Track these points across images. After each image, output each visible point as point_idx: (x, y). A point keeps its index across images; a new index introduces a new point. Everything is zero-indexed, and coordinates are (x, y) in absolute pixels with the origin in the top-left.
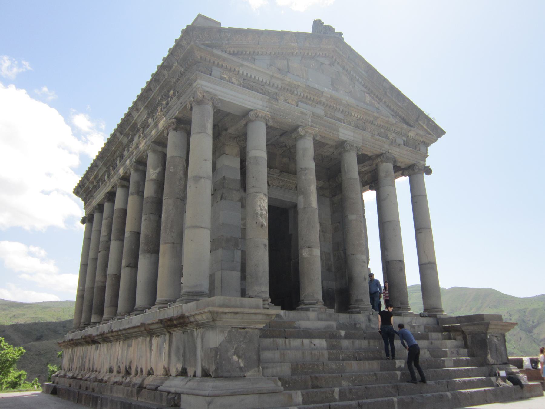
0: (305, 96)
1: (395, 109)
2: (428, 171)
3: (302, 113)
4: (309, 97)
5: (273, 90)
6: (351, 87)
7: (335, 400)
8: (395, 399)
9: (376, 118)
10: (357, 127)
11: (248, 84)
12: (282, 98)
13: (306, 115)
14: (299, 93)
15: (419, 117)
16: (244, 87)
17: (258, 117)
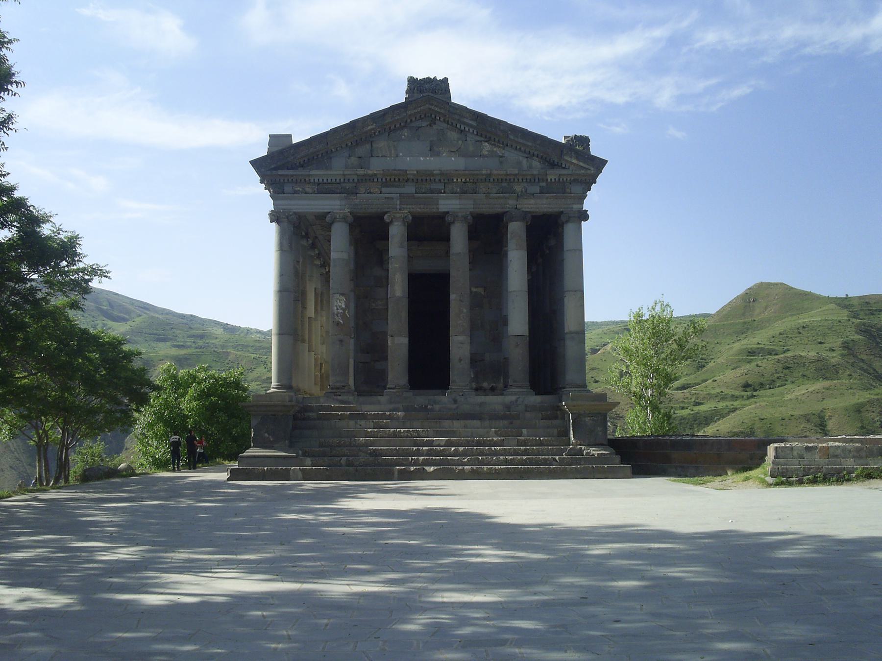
1: (527, 150)
2: (584, 216)
6: (460, 142)
9: (490, 175)
11: (324, 189)
12: (362, 190)
17: (335, 218)
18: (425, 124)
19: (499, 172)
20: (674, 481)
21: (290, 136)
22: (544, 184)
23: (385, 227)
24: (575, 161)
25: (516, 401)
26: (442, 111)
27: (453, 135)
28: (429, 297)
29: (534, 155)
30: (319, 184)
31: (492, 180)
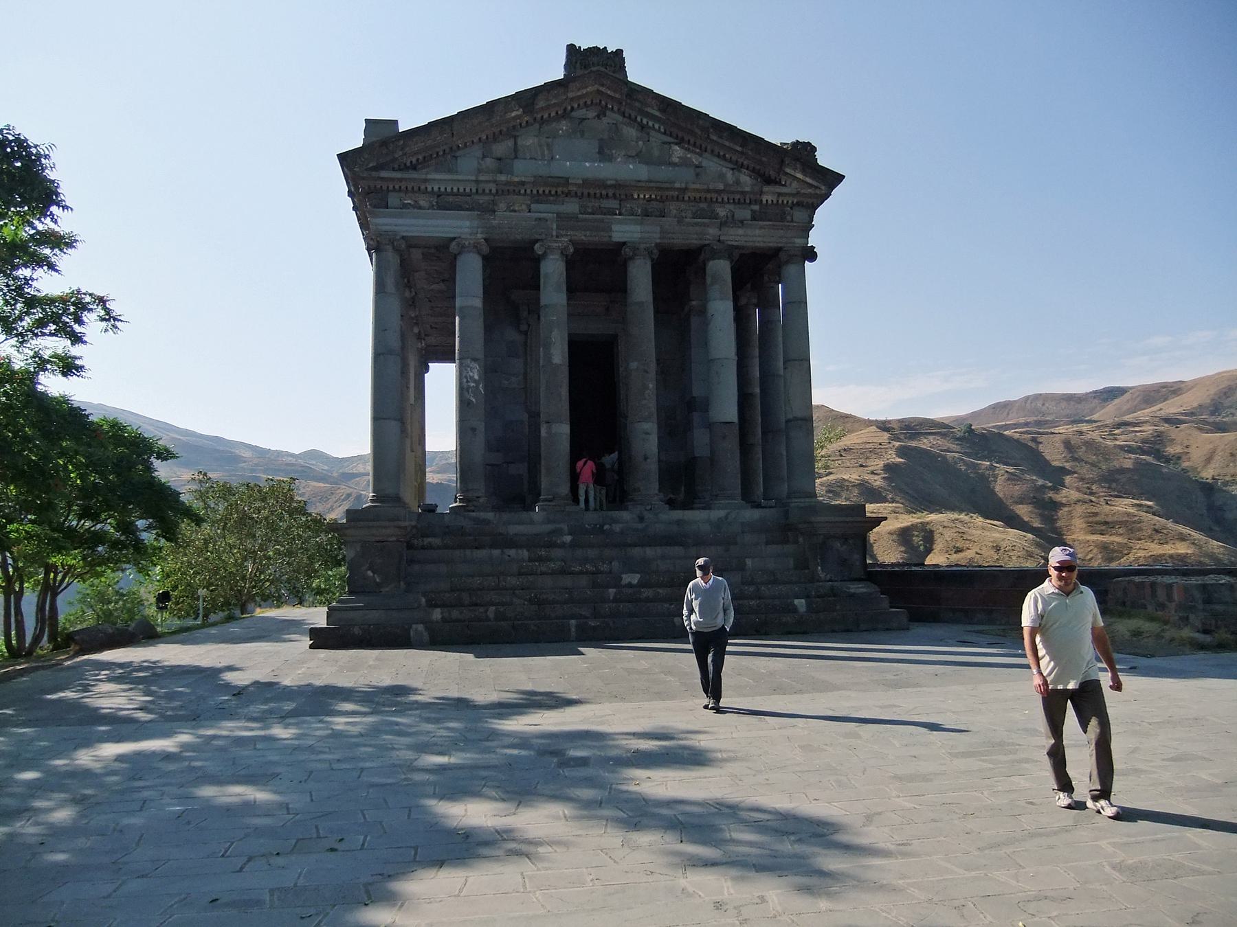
1: (734, 158)
2: (811, 255)
5: (486, 198)
6: (641, 143)
8: (573, 622)
9: (685, 190)
10: (646, 214)
11: (445, 202)
12: (502, 206)
16: (441, 207)
17: (463, 247)
18: (591, 114)
19: (698, 186)
21: (396, 122)
22: (756, 207)
24: (799, 176)
26: (617, 96)
27: (631, 132)
28: (595, 366)
29: (742, 166)
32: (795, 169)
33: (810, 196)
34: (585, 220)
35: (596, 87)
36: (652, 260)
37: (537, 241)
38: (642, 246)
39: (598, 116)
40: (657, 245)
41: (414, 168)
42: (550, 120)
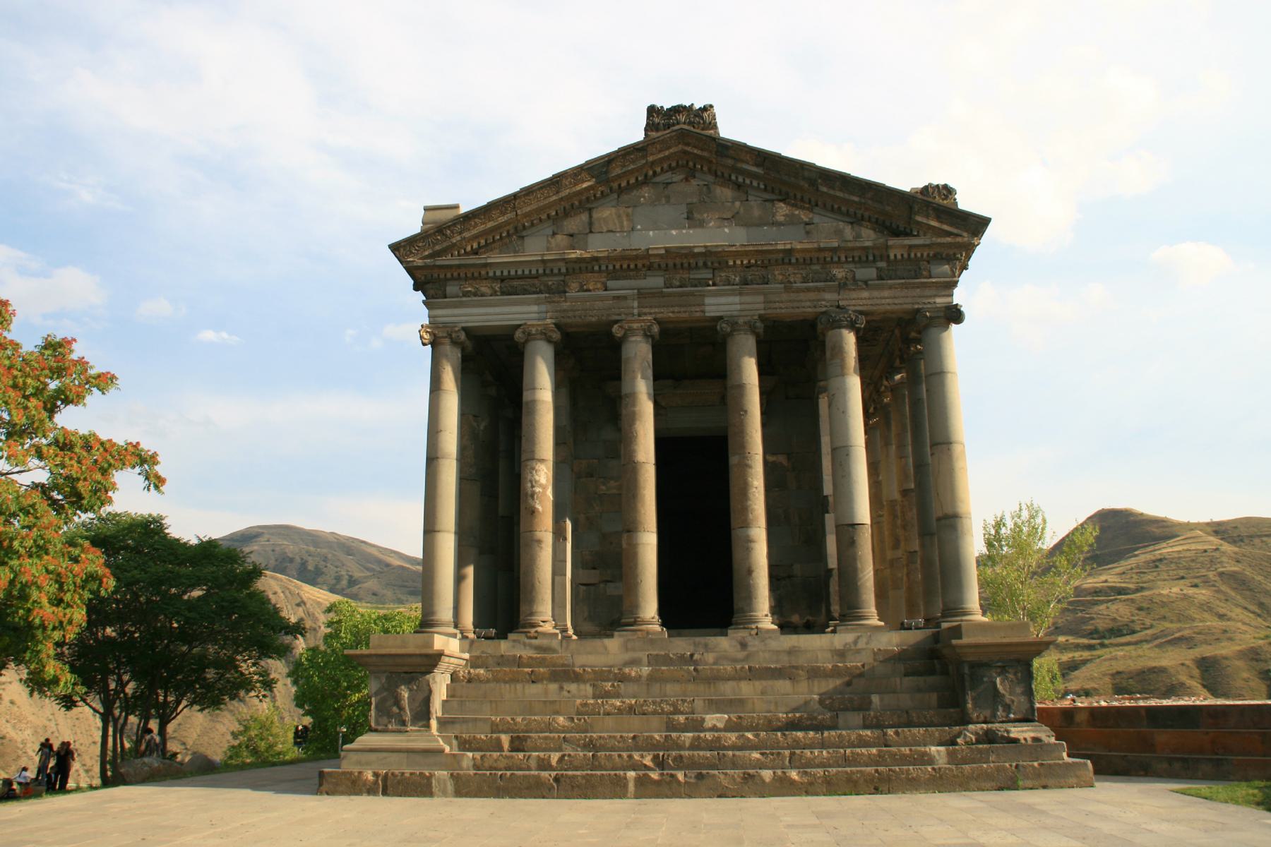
0: (618, 267)
1: (852, 210)
2: (955, 315)
3: (618, 298)
4: (625, 266)
6: (737, 204)
7: (529, 769)
8: (631, 774)
9: (789, 252)
10: (745, 282)
11: (511, 284)
12: (574, 285)
13: (625, 298)
14: (603, 268)
15: (911, 208)
16: (503, 293)
17: (529, 334)
20: (1183, 793)
21: (456, 207)
22: (883, 264)
23: (615, 346)
24: (934, 223)
25: (856, 642)
26: (705, 154)
29: (863, 218)
30: (502, 281)
31: (793, 261)
32: (927, 217)
33: (950, 245)
34: (670, 295)
35: (680, 147)
36: (757, 335)
37: (616, 322)
38: (741, 321)
39: (687, 180)
40: (760, 316)
41: (475, 252)
42: (630, 187)
